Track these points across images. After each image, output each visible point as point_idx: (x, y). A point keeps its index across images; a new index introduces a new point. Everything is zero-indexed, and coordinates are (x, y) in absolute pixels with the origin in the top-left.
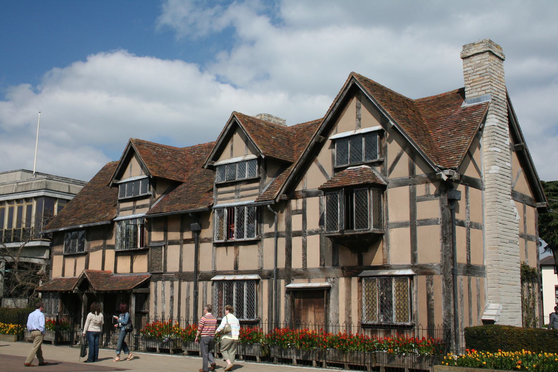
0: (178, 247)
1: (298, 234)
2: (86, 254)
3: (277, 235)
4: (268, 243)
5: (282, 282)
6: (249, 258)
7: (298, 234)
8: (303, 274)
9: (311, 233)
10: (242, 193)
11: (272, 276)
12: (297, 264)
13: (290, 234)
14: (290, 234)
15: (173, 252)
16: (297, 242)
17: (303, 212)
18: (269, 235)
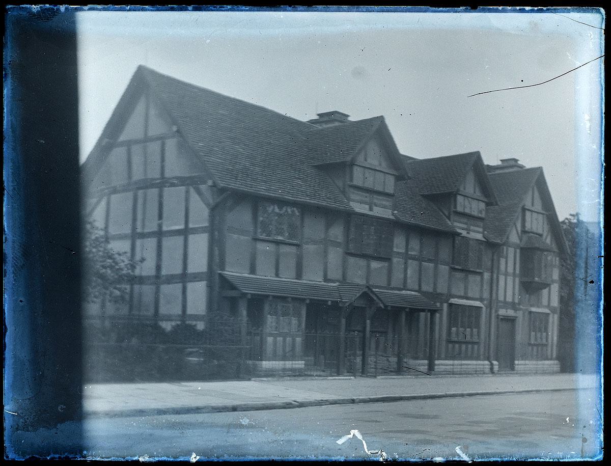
0: (415, 263)
4: (487, 276)
8: (506, 305)
12: (501, 298)
17: (506, 258)
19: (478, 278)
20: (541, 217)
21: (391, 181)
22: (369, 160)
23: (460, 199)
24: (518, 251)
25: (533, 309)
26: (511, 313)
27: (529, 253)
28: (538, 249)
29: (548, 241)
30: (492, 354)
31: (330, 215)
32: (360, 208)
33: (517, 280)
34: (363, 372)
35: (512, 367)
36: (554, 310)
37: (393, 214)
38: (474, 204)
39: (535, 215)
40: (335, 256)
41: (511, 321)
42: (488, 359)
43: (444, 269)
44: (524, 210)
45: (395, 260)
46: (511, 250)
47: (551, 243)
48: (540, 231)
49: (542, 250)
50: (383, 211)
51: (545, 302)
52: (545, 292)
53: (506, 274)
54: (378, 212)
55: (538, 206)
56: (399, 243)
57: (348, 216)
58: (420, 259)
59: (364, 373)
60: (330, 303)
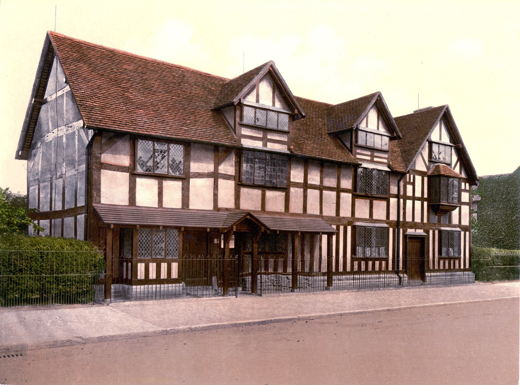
0: (317, 192)
1: (409, 198)
2: (185, 178)
3: (398, 196)
5: (401, 230)
6: (380, 211)
7: (409, 198)
8: (414, 225)
9: (418, 199)
10: (375, 159)
11: (397, 225)
12: (409, 219)
13: (406, 198)
14: (406, 198)
15: (313, 194)
16: (409, 203)
17: (413, 184)
18: (395, 196)
19: (384, 203)
20: (448, 149)
21: (285, 119)
22: (261, 102)
23: (360, 134)
24: (426, 179)
25: (443, 228)
26: (420, 232)
27: (436, 180)
28: (444, 176)
29: (457, 170)
30: (401, 269)
31: (219, 151)
32: (246, 143)
33: (425, 203)
34: (253, 291)
35: (423, 278)
36: (465, 229)
37: (289, 149)
38: (378, 138)
39: (442, 148)
40: (227, 188)
41: (422, 241)
42: (397, 273)
43: (346, 197)
44: (431, 143)
45: (292, 190)
46: (418, 178)
47: (461, 173)
48: (448, 160)
49: (449, 177)
50: (277, 146)
51: (455, 221)
52: (455, 213)
53: (414, 198)
54: (271, 147)
55: (446, 139)
56: (297, 175)
57: (240, 152)
58: (321, 188)
59: (254, 290)
60: (208, 230)
